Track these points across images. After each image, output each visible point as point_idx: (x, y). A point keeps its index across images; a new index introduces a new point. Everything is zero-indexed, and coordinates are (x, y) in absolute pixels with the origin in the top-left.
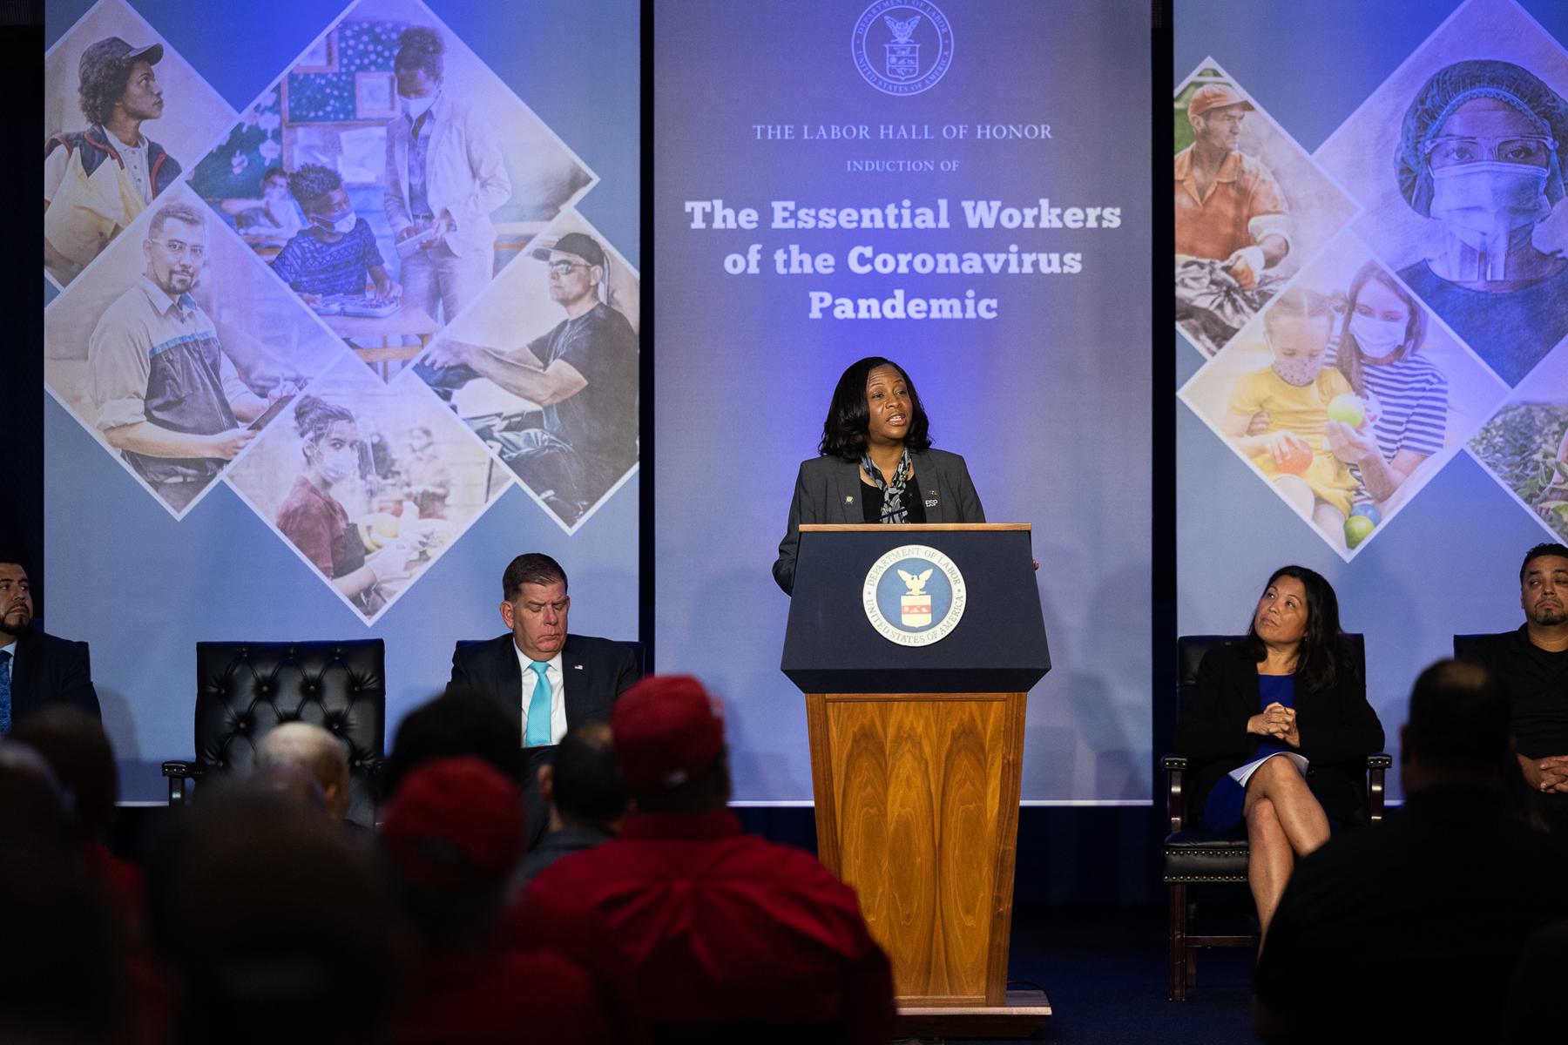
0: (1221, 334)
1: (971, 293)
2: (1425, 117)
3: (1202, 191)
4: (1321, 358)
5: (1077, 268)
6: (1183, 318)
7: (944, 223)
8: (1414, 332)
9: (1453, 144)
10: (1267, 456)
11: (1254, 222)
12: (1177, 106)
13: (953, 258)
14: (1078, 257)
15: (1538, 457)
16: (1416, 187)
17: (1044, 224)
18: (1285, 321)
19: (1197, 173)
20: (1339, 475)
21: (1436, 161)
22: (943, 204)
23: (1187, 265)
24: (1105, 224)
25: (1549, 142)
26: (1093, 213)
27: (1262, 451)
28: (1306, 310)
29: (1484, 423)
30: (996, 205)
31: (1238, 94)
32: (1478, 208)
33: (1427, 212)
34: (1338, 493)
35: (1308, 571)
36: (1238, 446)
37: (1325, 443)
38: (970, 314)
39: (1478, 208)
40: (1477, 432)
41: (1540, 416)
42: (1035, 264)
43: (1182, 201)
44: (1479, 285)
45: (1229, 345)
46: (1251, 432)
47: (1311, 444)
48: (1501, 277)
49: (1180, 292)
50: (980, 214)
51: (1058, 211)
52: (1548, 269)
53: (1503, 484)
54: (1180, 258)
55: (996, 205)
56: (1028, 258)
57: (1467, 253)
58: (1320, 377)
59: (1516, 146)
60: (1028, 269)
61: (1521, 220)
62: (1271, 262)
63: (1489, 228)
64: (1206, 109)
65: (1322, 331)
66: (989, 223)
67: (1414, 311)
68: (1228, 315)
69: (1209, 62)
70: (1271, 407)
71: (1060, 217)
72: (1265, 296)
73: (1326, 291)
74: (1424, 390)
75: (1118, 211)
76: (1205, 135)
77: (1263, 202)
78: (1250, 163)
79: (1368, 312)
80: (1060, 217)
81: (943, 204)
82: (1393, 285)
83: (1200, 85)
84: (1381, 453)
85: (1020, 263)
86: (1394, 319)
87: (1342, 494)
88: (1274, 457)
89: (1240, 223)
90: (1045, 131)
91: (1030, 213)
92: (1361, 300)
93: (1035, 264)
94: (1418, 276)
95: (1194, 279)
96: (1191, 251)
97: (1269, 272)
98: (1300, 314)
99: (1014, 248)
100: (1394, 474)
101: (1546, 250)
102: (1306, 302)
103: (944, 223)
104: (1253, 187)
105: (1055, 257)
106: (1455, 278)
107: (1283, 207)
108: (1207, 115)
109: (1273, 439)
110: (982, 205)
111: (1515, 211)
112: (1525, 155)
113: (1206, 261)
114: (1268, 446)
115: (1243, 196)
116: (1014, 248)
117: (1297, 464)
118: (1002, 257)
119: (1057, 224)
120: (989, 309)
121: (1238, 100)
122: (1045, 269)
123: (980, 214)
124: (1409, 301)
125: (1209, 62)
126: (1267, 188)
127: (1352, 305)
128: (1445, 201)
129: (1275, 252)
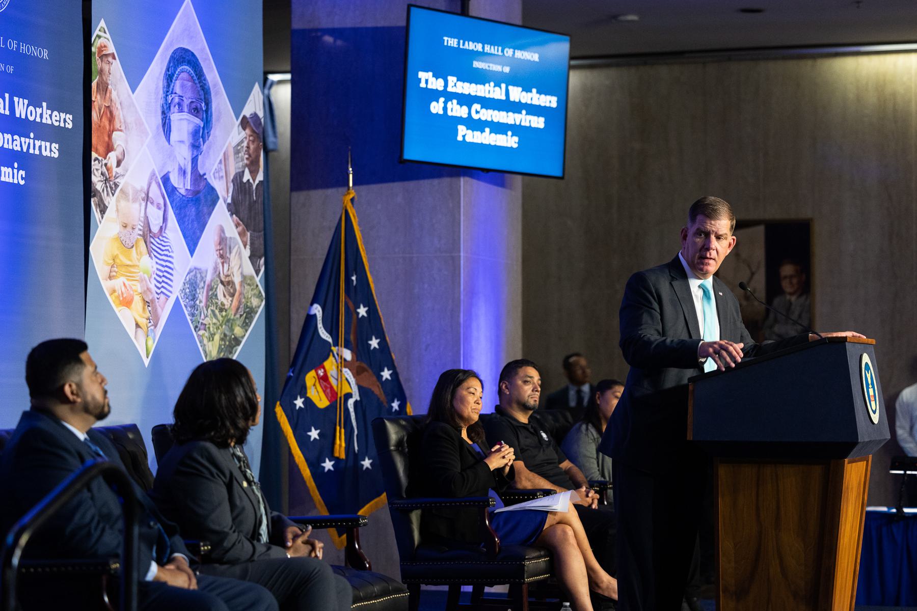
0: (103, 210)
1: (16, 165)
2: (169, 78)
3: (100, 110)
4: (137, 231)
5: (56, 156)
6: (94, 196)
7: (7, 113)
8: (165, 219)
9: (177, 100)
10: (116, 294)
11: (115, 135)
12: (93, 49)
13: (9, 136)
14: (57, 146)
15: (198, 302)
16: (166, 126)
17: (44, 121)
18: (123, 203)
19: (99, 97)
20: (144, 308)
21: (172, 108)
22: (7, 95)
23: (96, 159)
24: (67, 126)
25: (203, 105)
26: (63, 115)
27: (114, 291)
28: (131, 197)
29: (183, 280)
30: (26, 101)
31: (111, 49)
32: (182, 142)
33: (169, 141)
34: (143, 322)
35: (501, 375)
36: (106, 285)
37: (138, 287)
38: (16, 182)
39: (182, 142)
40: (181, 286)
41: (199, 276)
42: (40, 147)
43: (95, 116)
44: (183, 192)
45: (105, 216)
46: (110, 278)
47: (134, 288)
48: (189, 188)
49: (94, 179)
50: (22, 108)
51: (49, 112)
52: (202, 184)
53: (189, 318)
54: (94, 155)
55: (26, 101)
56: (38, 143)
57: (180, 169)
58: (137, 242)
59: (193, 105)
60: (37, 152)
61: (195, 153)
62: (119, 164)
63: (184, 154)
64: (103, 57)
65: (135, 211)
66: (23, 117)
67: (165, 205)
68: (104, 195)
69: (102, 24)
70: (118, 261)
71: (51, 116)
72: (116, 185)
73: (139, 188)
74: (166, 255)
75: (71, 117)
76: (101, 72)
77: (117, 125)
78: (114, 95)
79: (152, 203)
80: (51, 116)
81: (7, 95)
82: (159, 185)
83: (99, 37)
84: (156, 296)
85: (34, 149)
86: (159, 209)
87: (145, 321)
88: (118, 297)
89: (110, 136)
90: (45, 54)
91: (39, 111)
92: (150, 195)
93: (40, 147)
94: (166, 179)
95: (97, 170)
96: (97, 152)
97: (120, 170)
98: (128, 200)
99: (32, 135)
100: (159, 309)
101: (202, 173)
102: (131, 192)
103: (7, 113)
104: (115, 113)
105: (48, 144)
106: (176, 185)
107: (123, 128)
108: (101, 57)
109: (118, 283)
110: (21, 100)
111: (196, 146)
112: (195, 111)
113: (100, 158)
114: (116, 288)
115: (111, 119)
116: (32, 135)
117: (127, 303)
118: (27, 140)
119: (49, 122)
120: (22, 178)
121: (110, 52)
122: (44, 154)
123: (22, 108)
124: (164, 198)
125: (102, 24)
126: (119, 113)
127: (147, 198)
128: (174, 136)
129: (120, 157)
